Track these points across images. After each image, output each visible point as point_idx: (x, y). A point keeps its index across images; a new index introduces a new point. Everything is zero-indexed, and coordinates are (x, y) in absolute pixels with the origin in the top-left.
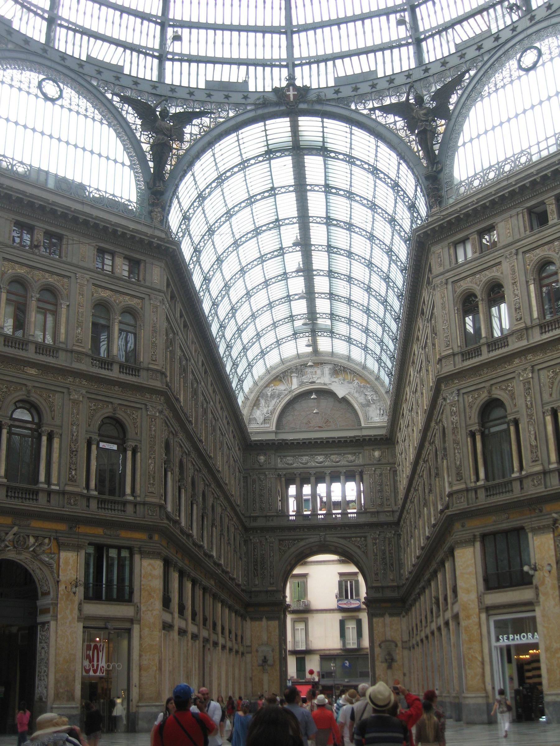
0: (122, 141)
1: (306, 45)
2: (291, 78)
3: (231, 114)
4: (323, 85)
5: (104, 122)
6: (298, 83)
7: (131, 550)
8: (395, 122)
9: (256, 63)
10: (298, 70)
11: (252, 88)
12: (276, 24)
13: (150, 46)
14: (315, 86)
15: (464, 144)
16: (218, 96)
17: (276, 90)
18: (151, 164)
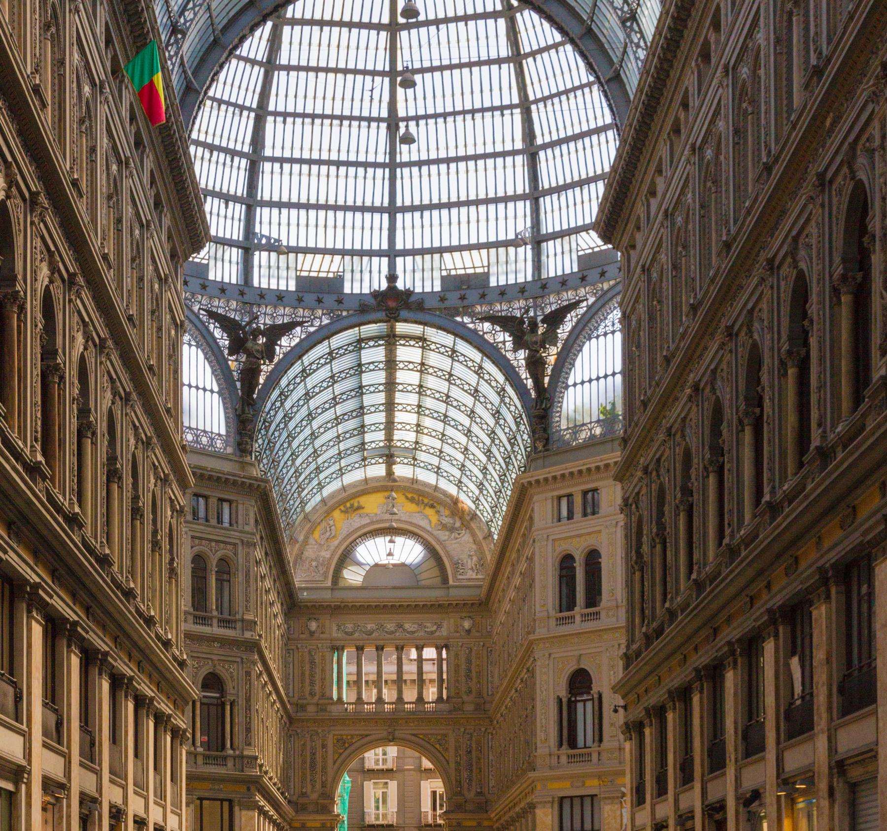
0: (210, 362)
1: (411, 232)
2: (392, 278)
3: (326, 321)
4: (428, 289)
5: (193, 343)
6: (400, 285)
7: (230, 802)
8: (504, 342)
9: (352, 253)
10: (399, 261)
11: (347, 290)
12: (377, 203)
13: (235, 237)
14: (418, 290)
15: (575, 385)
16: (310, 298)
17: (376, 294)
18: (238, 384)
